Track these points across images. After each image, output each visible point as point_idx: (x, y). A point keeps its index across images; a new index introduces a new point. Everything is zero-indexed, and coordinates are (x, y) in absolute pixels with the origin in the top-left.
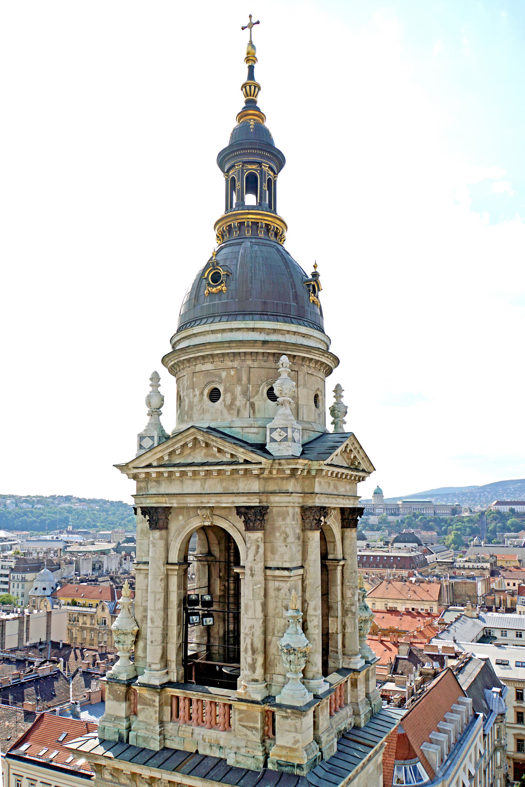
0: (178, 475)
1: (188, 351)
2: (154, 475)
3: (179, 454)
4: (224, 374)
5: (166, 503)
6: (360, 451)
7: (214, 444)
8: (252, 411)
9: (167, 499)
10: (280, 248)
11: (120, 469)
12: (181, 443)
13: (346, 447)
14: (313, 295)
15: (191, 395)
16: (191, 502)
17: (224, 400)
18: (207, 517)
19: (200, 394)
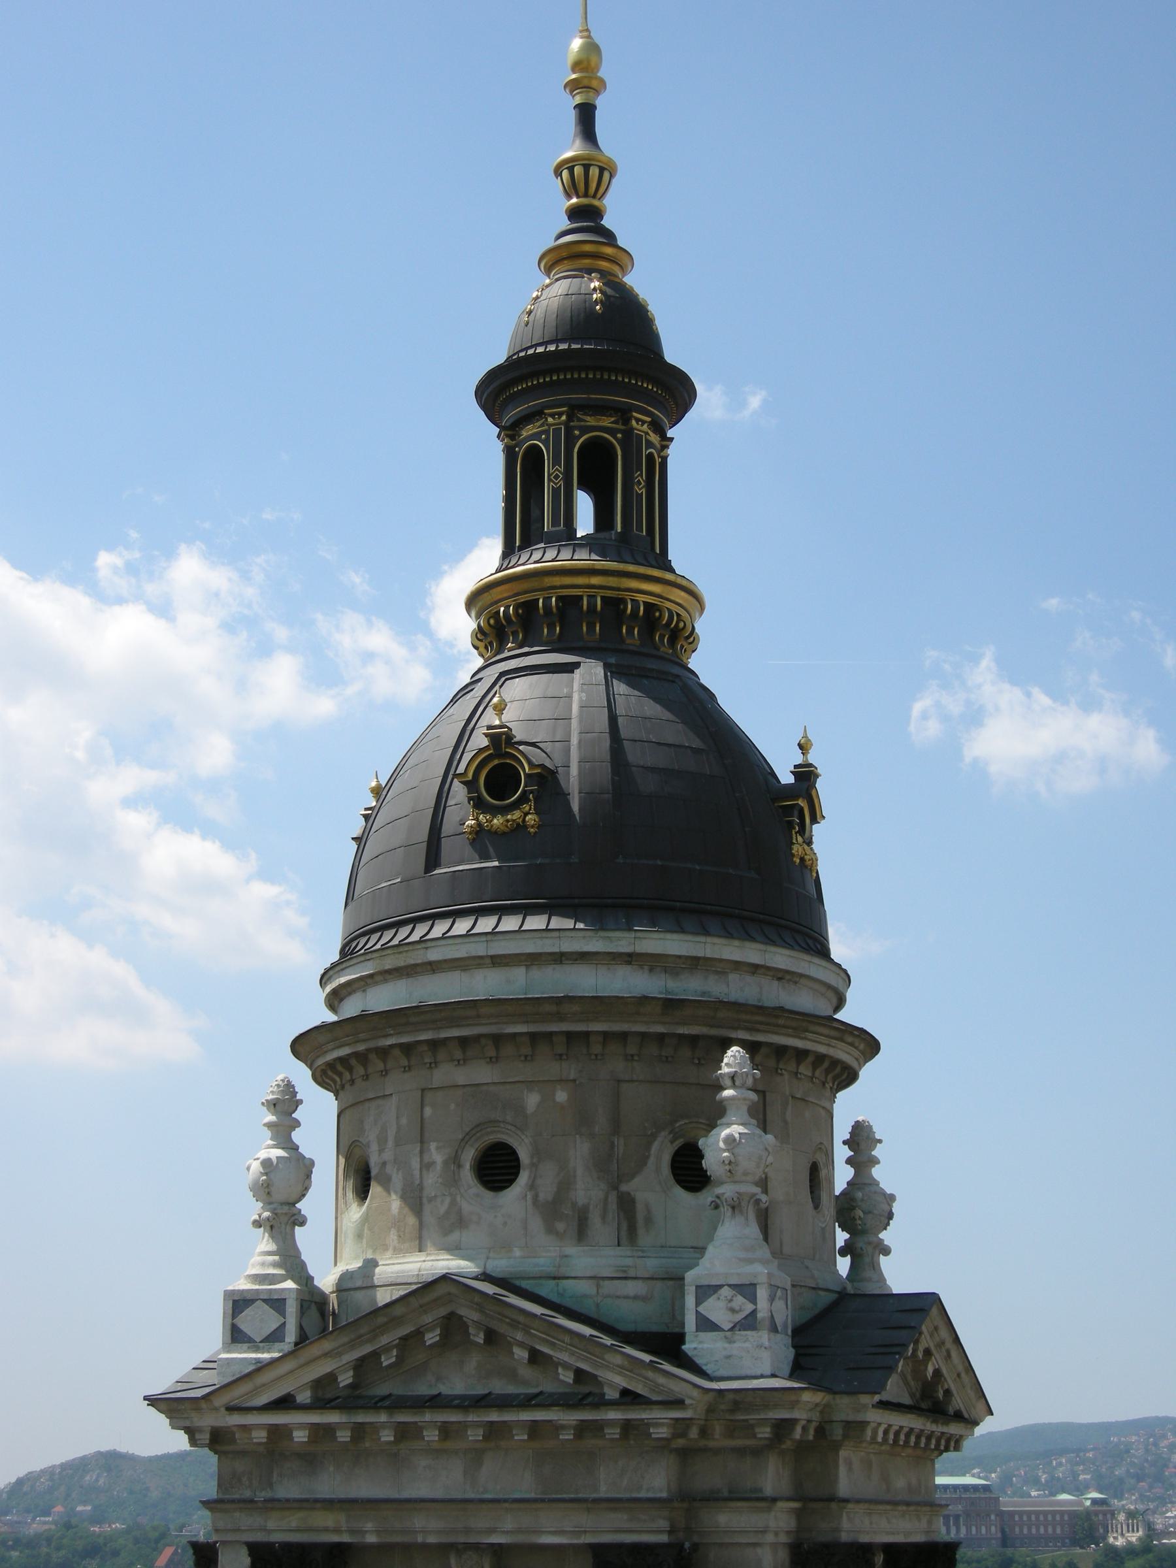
0: (387, 1436)
3: (390, 1366)
4: (532, 1100)
5: (337, 1531)
6: (954, 1354)
7: (519, 1336)
8: (624, 1226)
15: (415, 1163)
17: (532, 1186)
19: (446, 1163)
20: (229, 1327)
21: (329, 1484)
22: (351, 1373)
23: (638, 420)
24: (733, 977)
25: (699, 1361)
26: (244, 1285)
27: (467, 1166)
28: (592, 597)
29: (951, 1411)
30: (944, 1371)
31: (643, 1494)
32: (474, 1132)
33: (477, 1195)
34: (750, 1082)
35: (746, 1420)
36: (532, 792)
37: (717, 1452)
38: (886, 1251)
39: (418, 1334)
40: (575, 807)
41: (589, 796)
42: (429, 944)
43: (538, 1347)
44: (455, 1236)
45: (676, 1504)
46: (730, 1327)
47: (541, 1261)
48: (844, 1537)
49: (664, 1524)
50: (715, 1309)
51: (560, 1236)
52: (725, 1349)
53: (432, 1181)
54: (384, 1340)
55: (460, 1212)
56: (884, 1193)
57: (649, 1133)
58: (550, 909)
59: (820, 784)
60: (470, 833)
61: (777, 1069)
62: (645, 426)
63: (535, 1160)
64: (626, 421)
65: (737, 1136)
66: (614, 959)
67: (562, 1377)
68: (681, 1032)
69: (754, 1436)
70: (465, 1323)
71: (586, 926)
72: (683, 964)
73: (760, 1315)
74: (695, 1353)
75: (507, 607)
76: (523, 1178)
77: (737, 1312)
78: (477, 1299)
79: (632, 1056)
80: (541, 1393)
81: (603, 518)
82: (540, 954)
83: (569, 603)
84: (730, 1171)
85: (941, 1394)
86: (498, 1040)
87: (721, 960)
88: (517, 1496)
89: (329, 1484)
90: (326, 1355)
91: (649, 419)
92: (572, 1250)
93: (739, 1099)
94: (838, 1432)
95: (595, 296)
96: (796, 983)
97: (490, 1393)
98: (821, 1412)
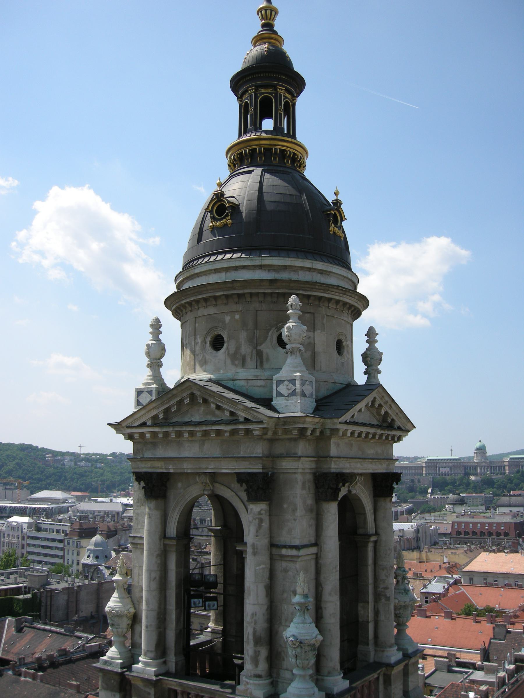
0: (173, 436)
1: (189, 293)
2: (148, 436)
4: (228, 319)
5: (162, 468)
6: (393, 406)
7: (212, 400)
8: (259, 361)
9: (163, 463)
10: (296, 175)
11: (115, 429)
12: (178, 399)
13: (373, 402)
14: (333, 225)
15: (193, 344)
16: (188, 467)
17: (227, 349)
19: (201, 342)
20: (136, 401)
21: (160, 452)
22: (163, 414)
23: (280, 89)
24: (301, 273)
25: (277, 408)
26: (141, 386)
27: (208, 343)
28: (260, 148)
29: (396, 427)
30: (390, 412)
31: (254, 455)
32: (210, 331)
33: (211, 353)
34: (298, 307)
35: (289, 428)
36: (229, 212)
37: (282, 440)
38: (380, 372)
40: (244, 216)
41: (249, 212)
42: (195, 267)
43: (218, 403)
44: (204, 367)
45: (264, 459)
46: (287, 395)
47: (229, 374)
48: (333, 470)
49: (260, 466)
50: (283, 389)
51: (236, 366)
52: (285, 403)
53: (198, 348)
55: (205, 359)
56: (378, 352)
57: (268, 328)
58: (234, 252)
60: (210, 228)
61: (319, 305)
62: (283, 91)
63: (228, 340)
64: (276, 90)
65: (291, 326)
66: (255, 268)
67: (226, 414)
68: (278, 292)
69: (292, 434)
70: (196, 395)
71: (245, 255)
72: (281, 268)
73: (297, 391)
74: (275, 405)
75: (234, 155)
77: (290, 390)
78: (198, 387)
79: (261, 301)
80: (222, 420)
82: (230, 267)
83: (253, 151)
84: (289, 339)
85: (389, 421)
86: (216, 298)
87: (295, 266)
88: (215, 456)
89: (160, 452)
90: (154, 408)
91: (284, 89)
93: (294, 314)
94: (328, 433)
95: (265, 50)
96: (328, 275)
97: (207, 420)
98: (322, 425)
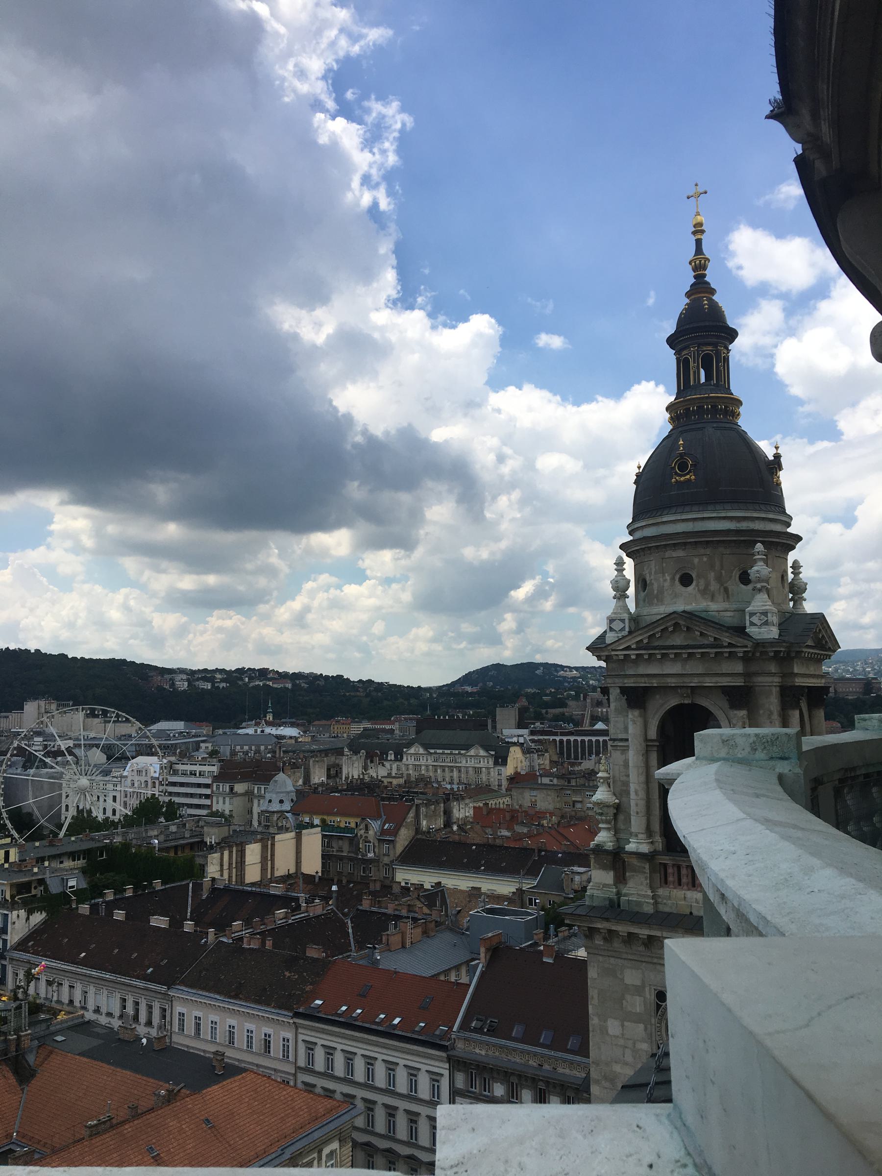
0: (659, 657)
4: (696, 560)
5: (645, 683)
9: (646, 679)
15: (661, 579)
16: (672, 682)
17: (697, 585)
18: (688, 696)
21: (642, 670)
39: (666, 628)
50: (755, 619)
54: (657, 630)
59: (782, 459)
76: (694, 583)
78: (684, 618)
81: (708, 377)
86: (685, 544)
89: (642, 670)
92: (710, 603)
94: (793, 654)
